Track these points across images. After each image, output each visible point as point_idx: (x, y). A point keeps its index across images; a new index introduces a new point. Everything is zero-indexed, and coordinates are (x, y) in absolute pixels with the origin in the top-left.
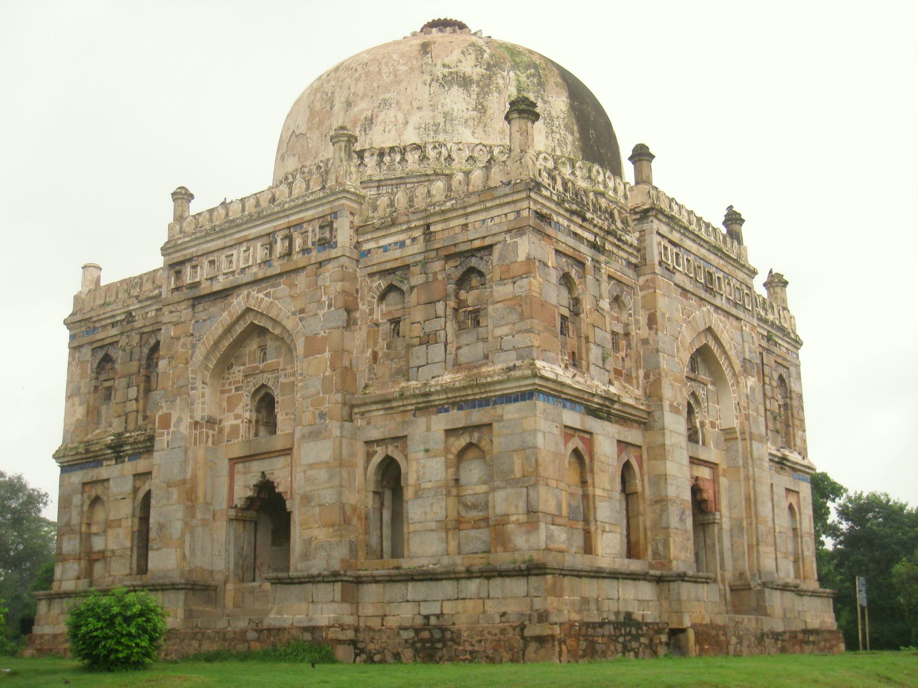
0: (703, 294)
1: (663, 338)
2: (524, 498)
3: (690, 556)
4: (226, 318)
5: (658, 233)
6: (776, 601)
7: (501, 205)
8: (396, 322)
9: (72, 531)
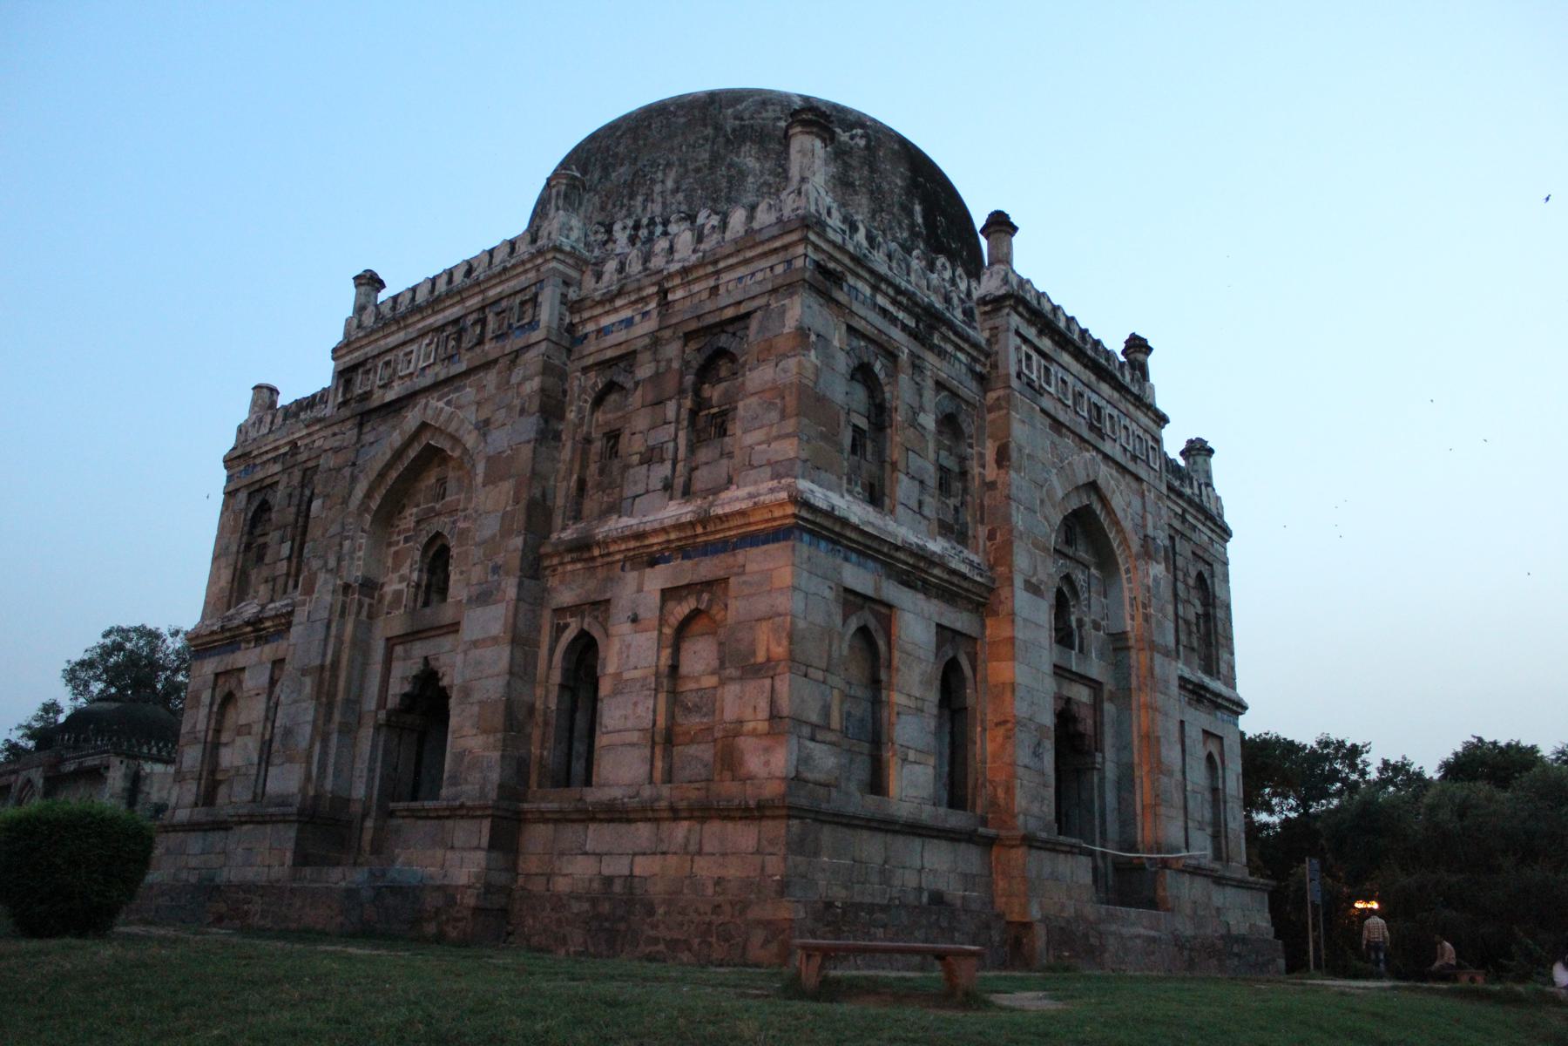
0: (1086, 434)
1: (1017, 481)
2: (767, 694)
3: (1049, 809)
4: (396, 439)
5: (1018, 333)
6: (1186, 891)
7: (764, 255)
8: (613, 436)
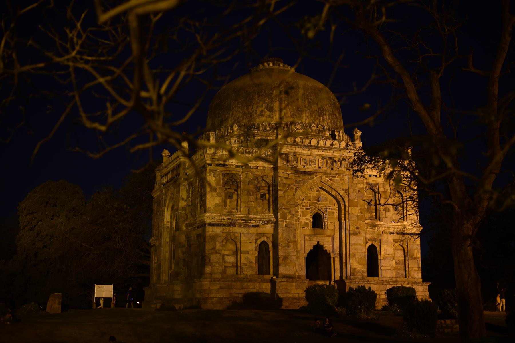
9: (217, 253)
